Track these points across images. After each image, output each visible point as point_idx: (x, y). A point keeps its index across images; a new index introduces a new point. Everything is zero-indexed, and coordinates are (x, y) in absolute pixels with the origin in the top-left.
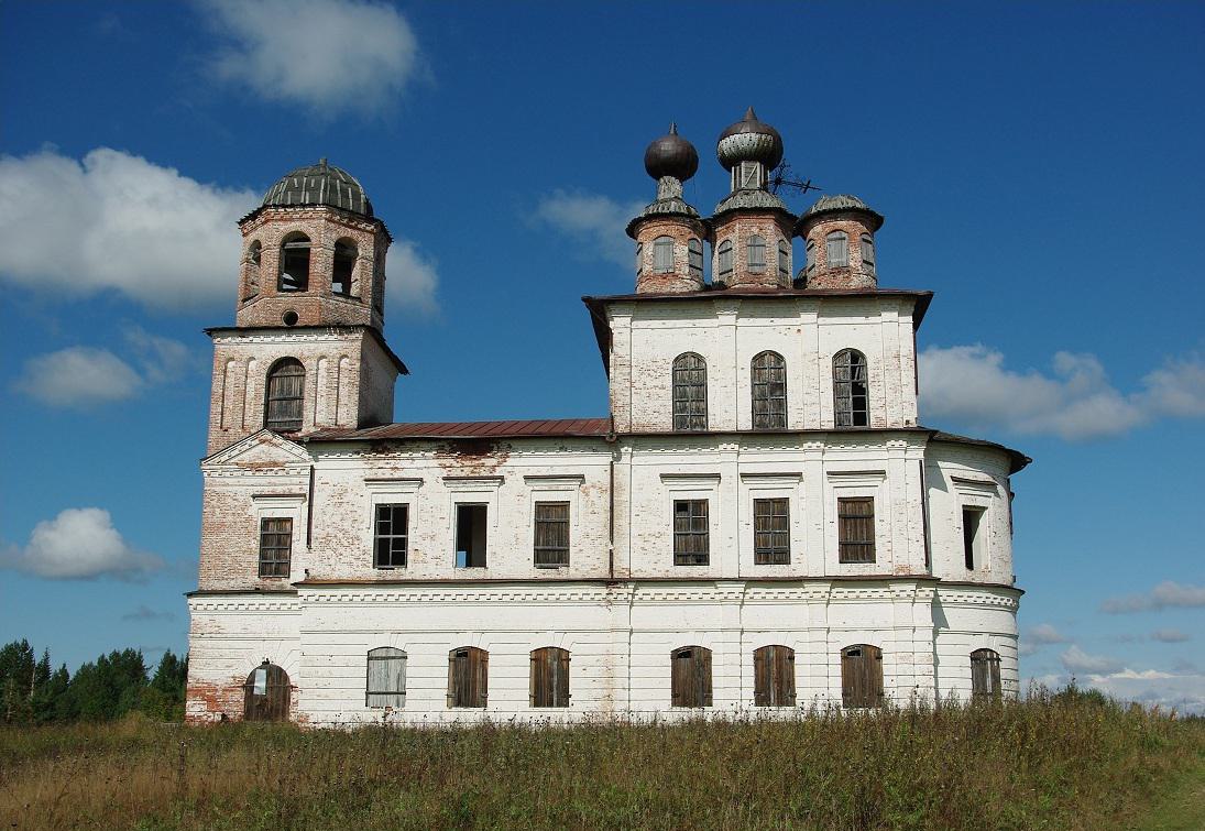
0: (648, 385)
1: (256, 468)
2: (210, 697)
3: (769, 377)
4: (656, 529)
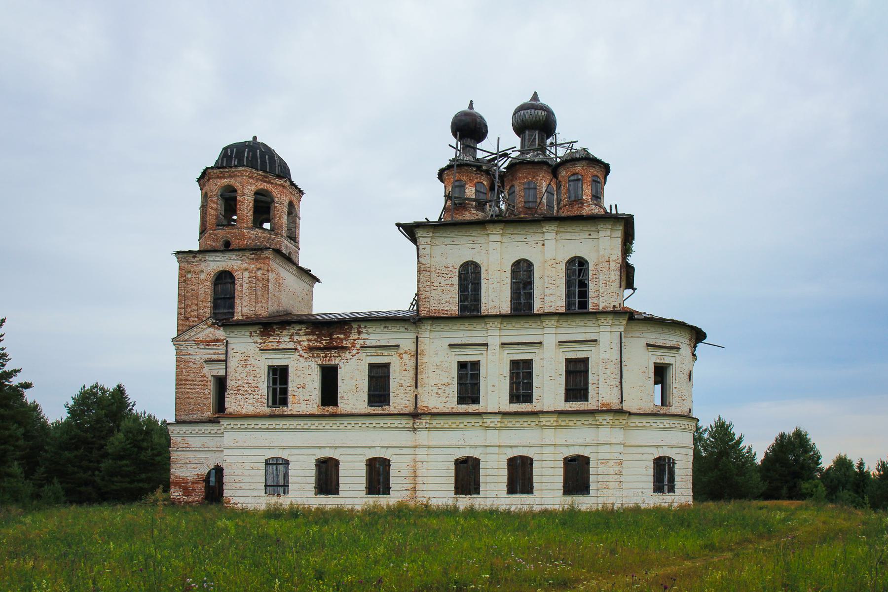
0: (443, 283)
3: (523, 276)
4: (446, 381)
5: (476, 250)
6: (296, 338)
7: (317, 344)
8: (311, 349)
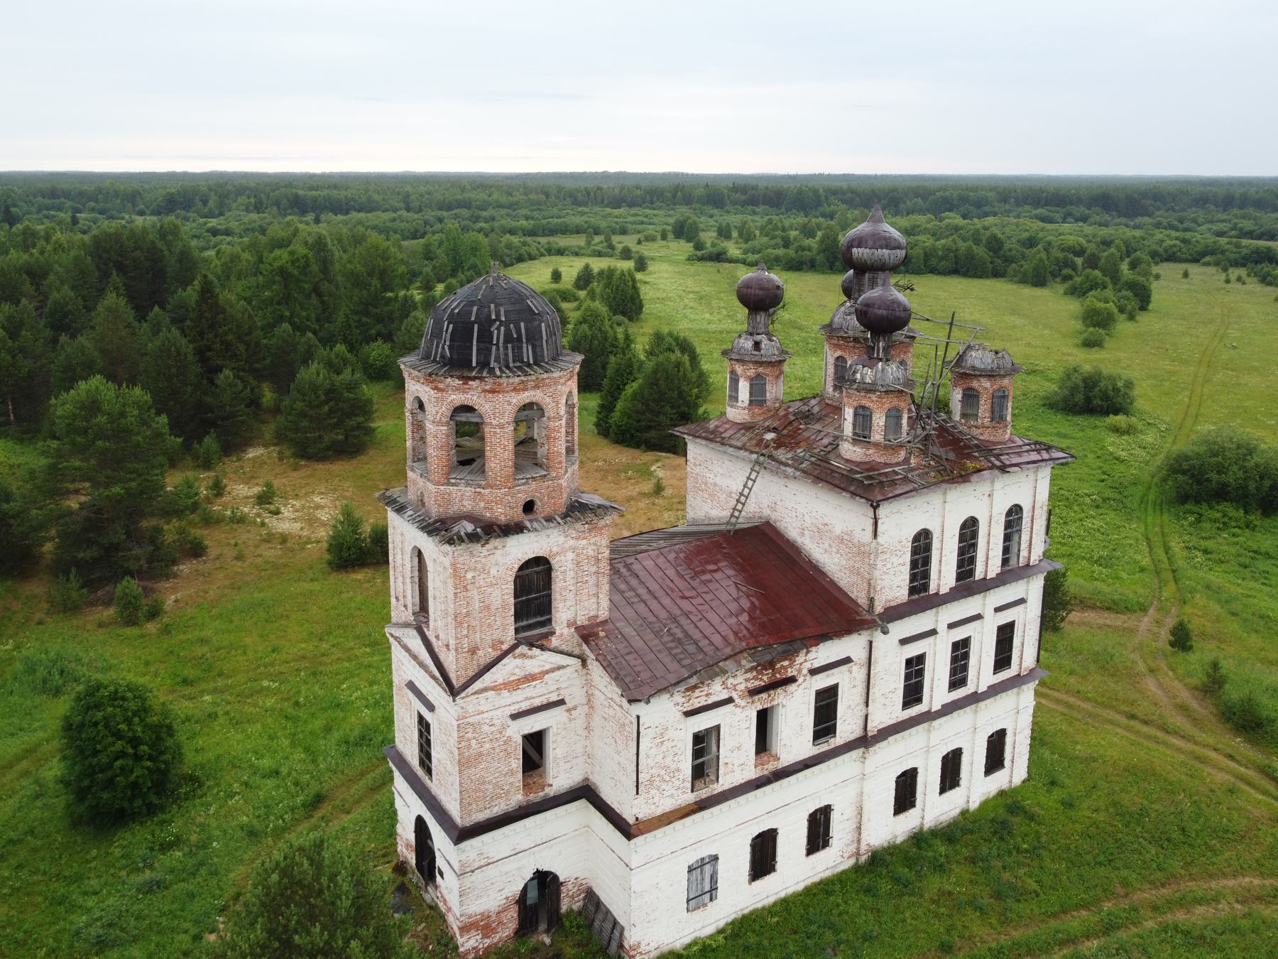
1: (512, 685)
2: (483, 925)
7: (757, 683)
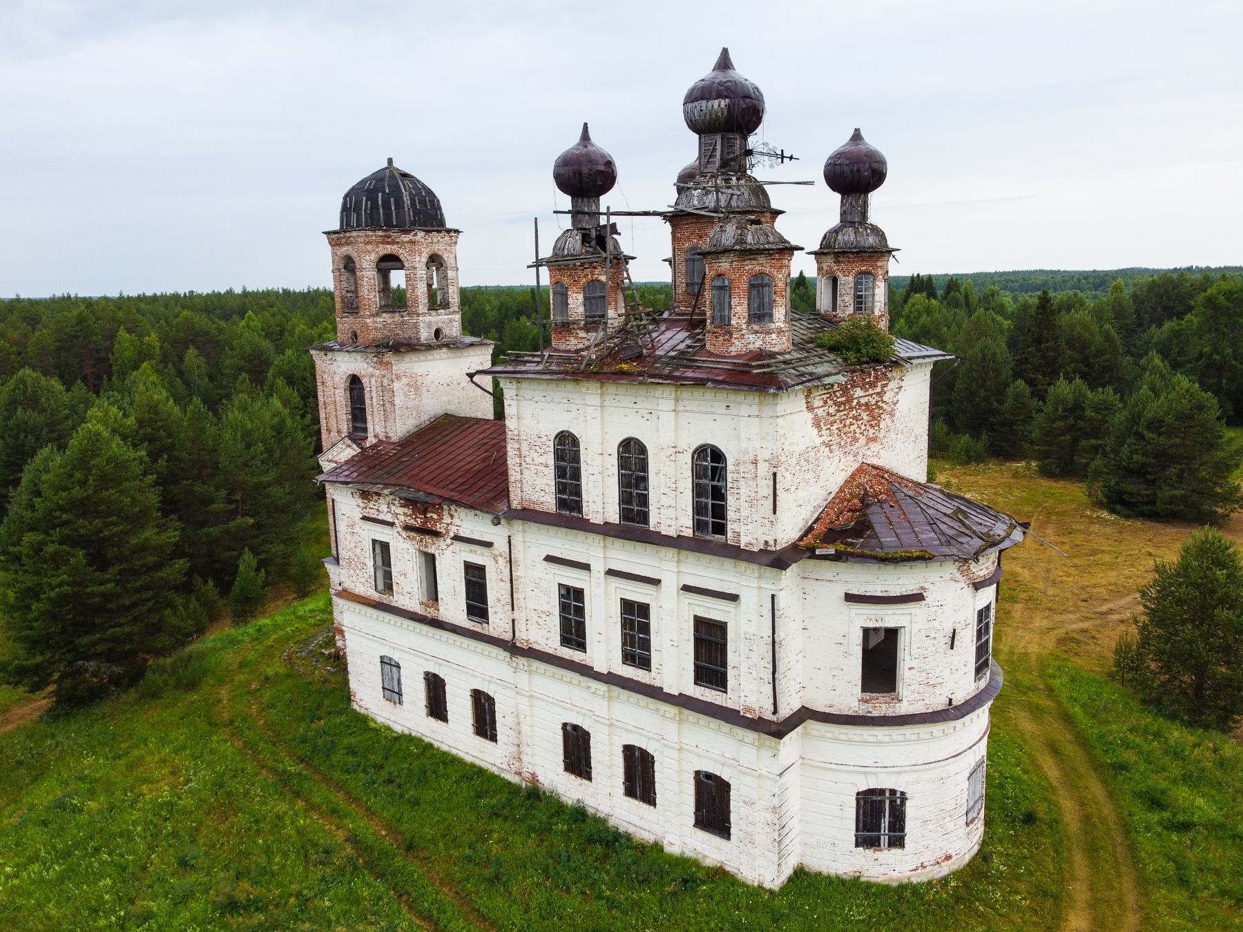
4: (546, 608)
5: (572, 415)
6: (393, 508)
7: (412, 522)
8: (408, 528)
